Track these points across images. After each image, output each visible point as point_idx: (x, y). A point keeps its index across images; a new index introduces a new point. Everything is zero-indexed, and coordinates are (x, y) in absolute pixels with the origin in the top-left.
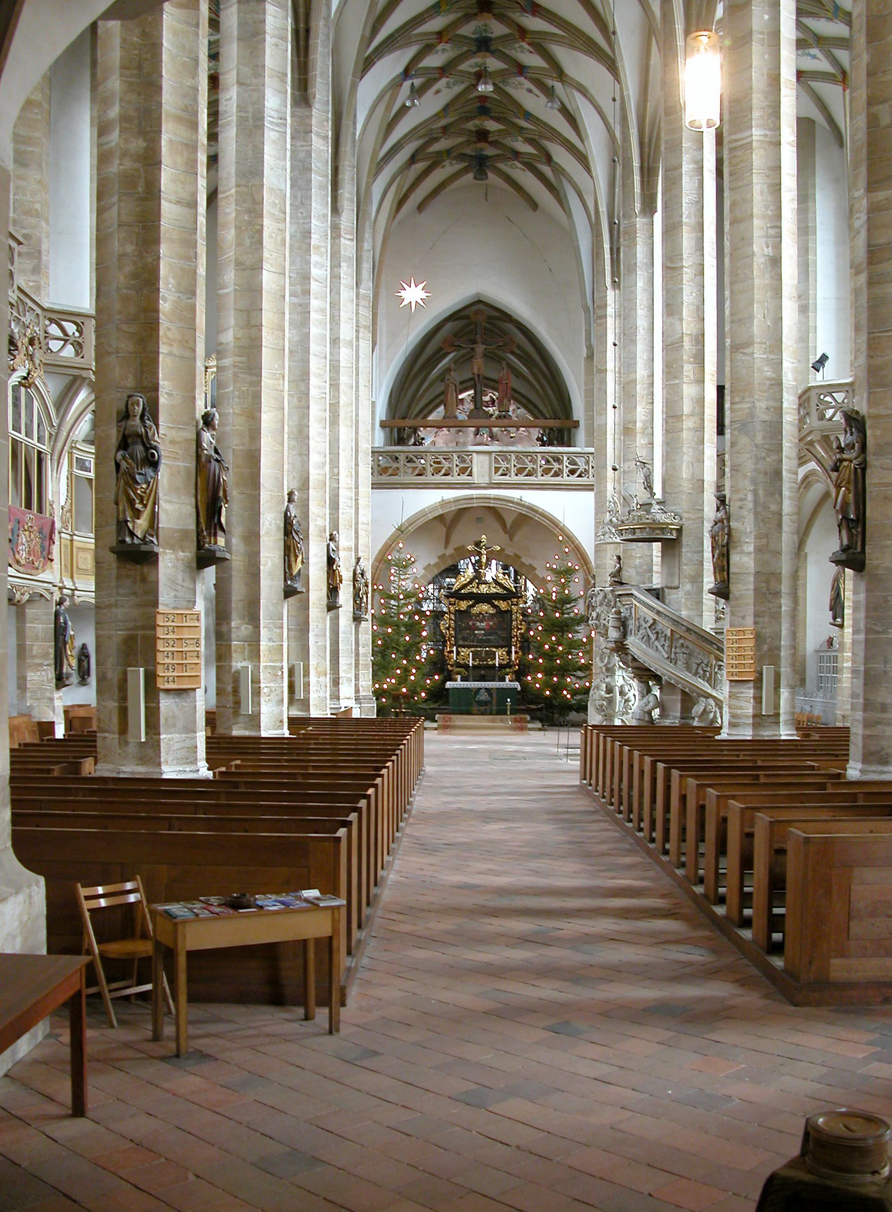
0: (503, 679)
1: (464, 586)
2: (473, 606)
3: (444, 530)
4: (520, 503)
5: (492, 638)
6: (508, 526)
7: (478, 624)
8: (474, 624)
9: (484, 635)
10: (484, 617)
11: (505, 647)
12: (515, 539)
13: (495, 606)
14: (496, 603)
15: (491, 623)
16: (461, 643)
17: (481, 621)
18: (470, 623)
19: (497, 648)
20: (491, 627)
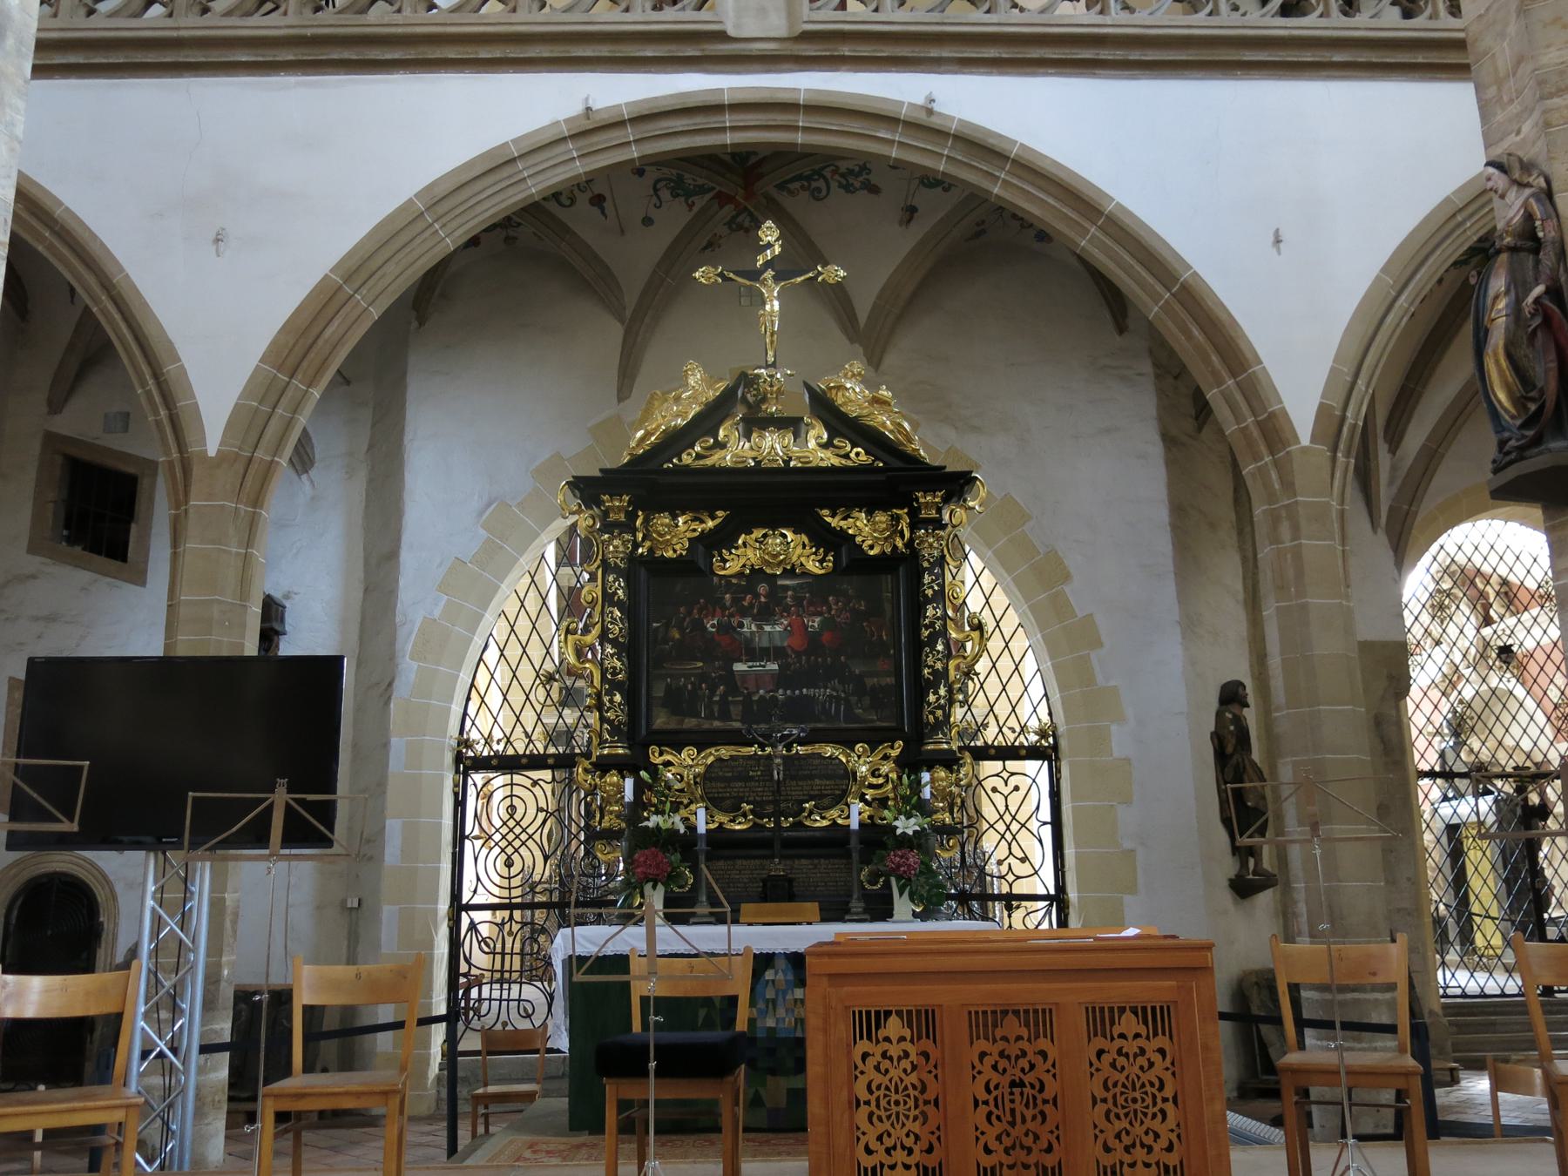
0: (881, 909)
1: (677, 440)
2: (721, 540)
3: (616, 331)
4: (924, 126)
5: (820, 693)
6: (862, 316)
7: (749, 627)
8: (724, 628)
9: (781, 679)
10: (776, 593)
11: (888, 736)
12: (891, 360)
13: (828, 540)
14: (834, 522)
15: (815, 623)
16: (661, 721)
17: (765, 615)
18: (711, 624)
19: (849, 744)
20: (813, 641)
